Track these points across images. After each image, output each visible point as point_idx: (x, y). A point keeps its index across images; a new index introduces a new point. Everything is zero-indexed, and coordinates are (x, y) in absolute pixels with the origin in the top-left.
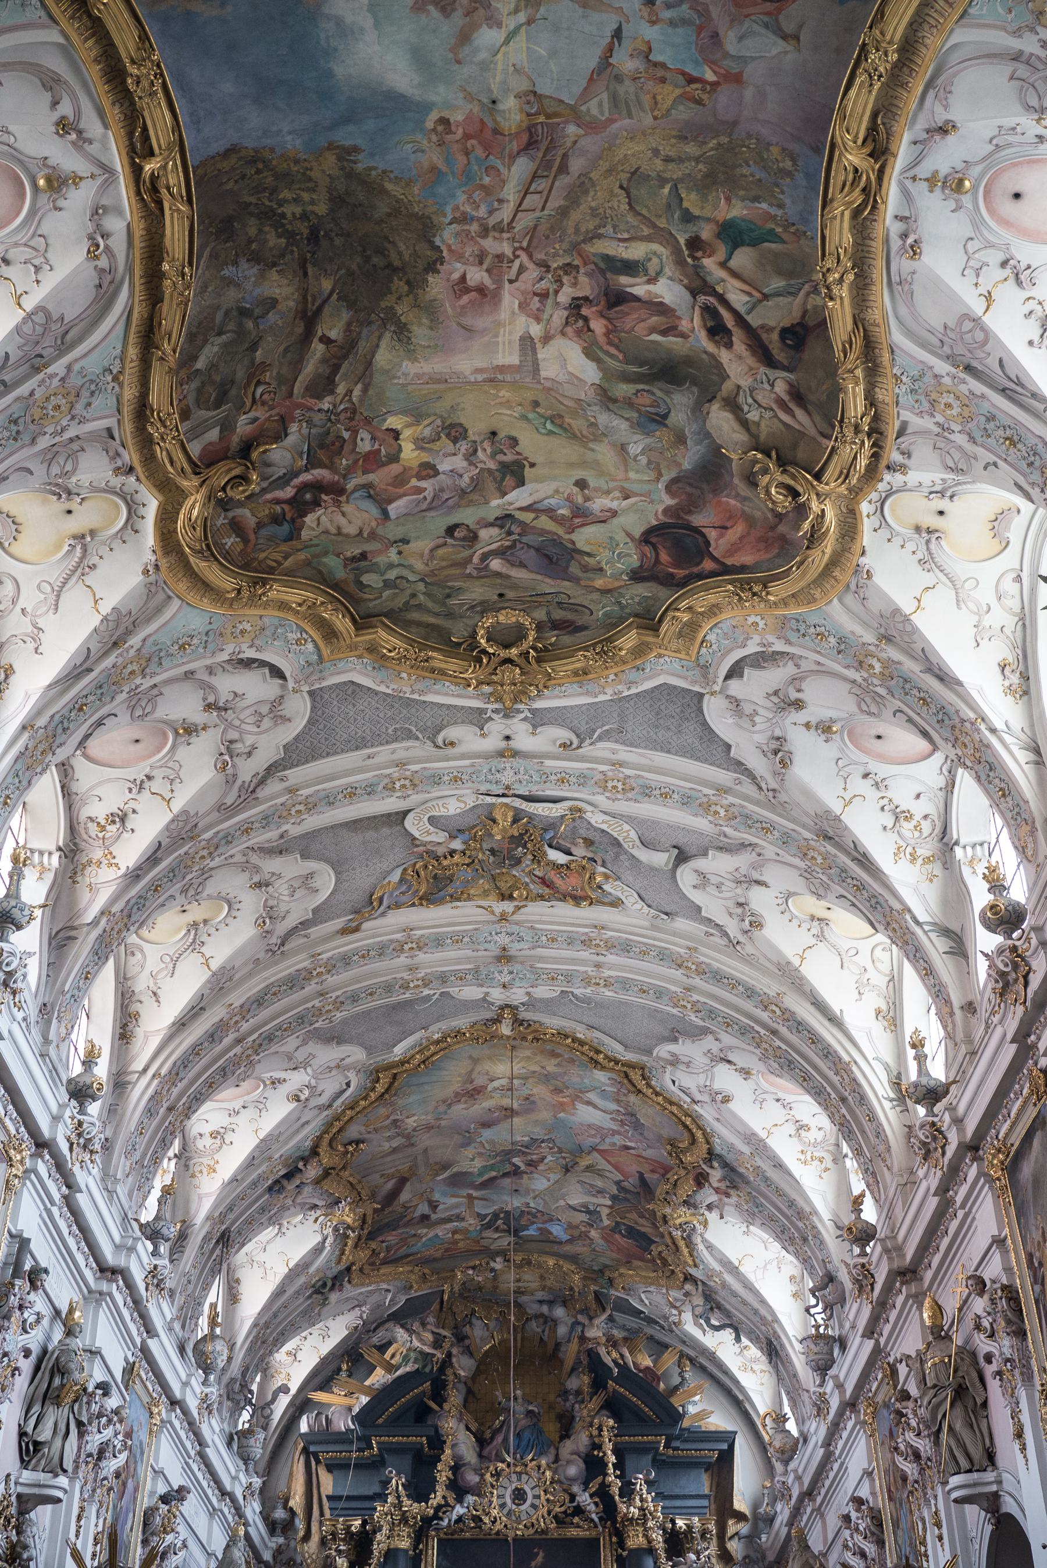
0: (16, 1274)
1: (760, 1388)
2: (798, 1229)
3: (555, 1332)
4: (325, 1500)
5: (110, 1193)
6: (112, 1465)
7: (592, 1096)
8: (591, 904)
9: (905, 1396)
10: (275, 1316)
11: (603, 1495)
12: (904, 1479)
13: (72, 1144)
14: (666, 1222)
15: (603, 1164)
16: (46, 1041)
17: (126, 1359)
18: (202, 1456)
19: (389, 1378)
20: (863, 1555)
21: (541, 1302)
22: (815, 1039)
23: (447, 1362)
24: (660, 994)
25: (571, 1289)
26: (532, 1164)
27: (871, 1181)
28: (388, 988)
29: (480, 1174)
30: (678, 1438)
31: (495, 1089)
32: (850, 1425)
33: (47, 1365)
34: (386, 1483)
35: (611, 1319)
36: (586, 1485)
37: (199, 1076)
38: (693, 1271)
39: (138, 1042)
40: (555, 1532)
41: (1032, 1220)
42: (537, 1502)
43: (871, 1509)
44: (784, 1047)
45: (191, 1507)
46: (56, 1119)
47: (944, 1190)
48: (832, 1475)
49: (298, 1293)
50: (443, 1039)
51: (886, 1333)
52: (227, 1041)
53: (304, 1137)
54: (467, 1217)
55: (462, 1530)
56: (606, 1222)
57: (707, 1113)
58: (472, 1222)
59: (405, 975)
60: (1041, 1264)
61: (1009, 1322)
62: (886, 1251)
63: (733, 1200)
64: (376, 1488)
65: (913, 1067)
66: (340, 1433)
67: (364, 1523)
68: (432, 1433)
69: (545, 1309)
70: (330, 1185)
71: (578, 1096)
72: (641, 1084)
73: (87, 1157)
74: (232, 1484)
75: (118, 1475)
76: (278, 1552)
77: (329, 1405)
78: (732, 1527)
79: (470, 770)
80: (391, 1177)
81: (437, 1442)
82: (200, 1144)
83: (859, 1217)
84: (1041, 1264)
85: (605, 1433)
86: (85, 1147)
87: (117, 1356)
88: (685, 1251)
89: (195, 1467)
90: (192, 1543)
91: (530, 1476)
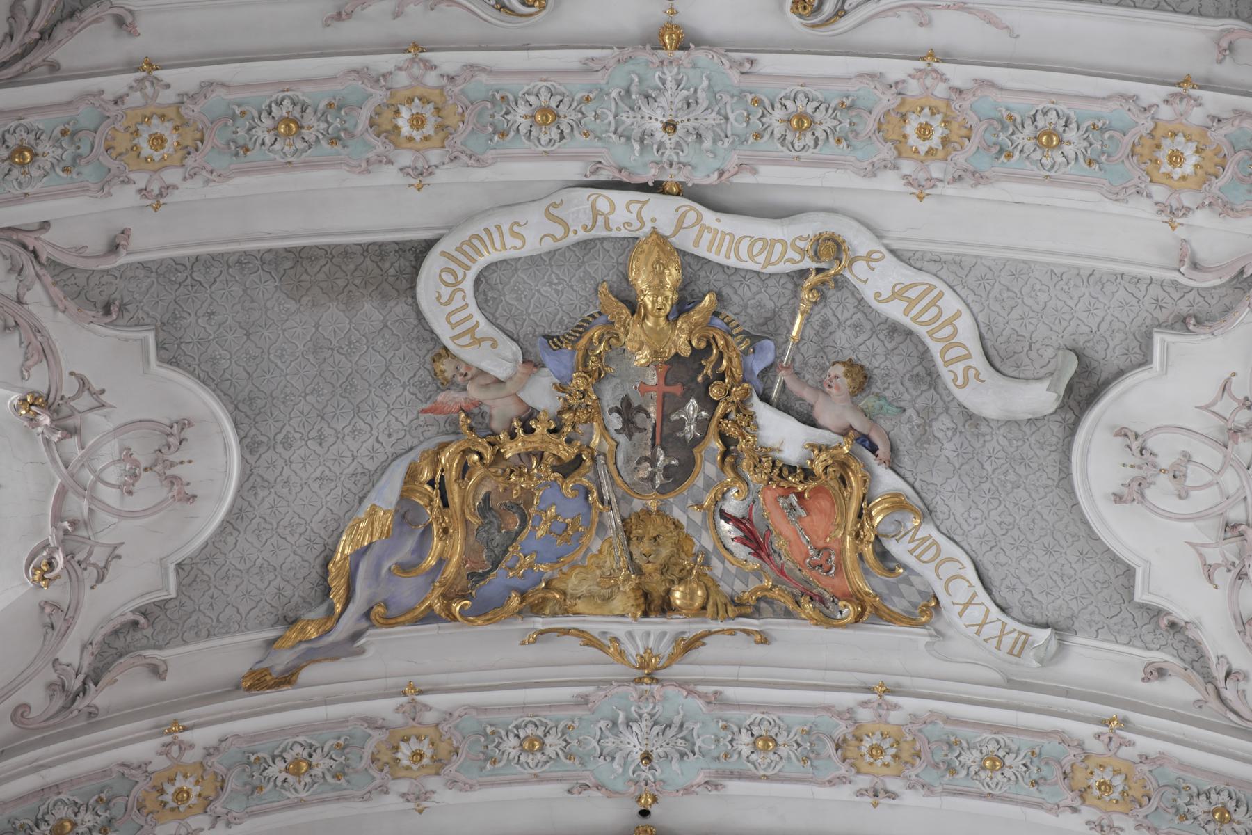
8: (858, 618)
79: (578, 87)
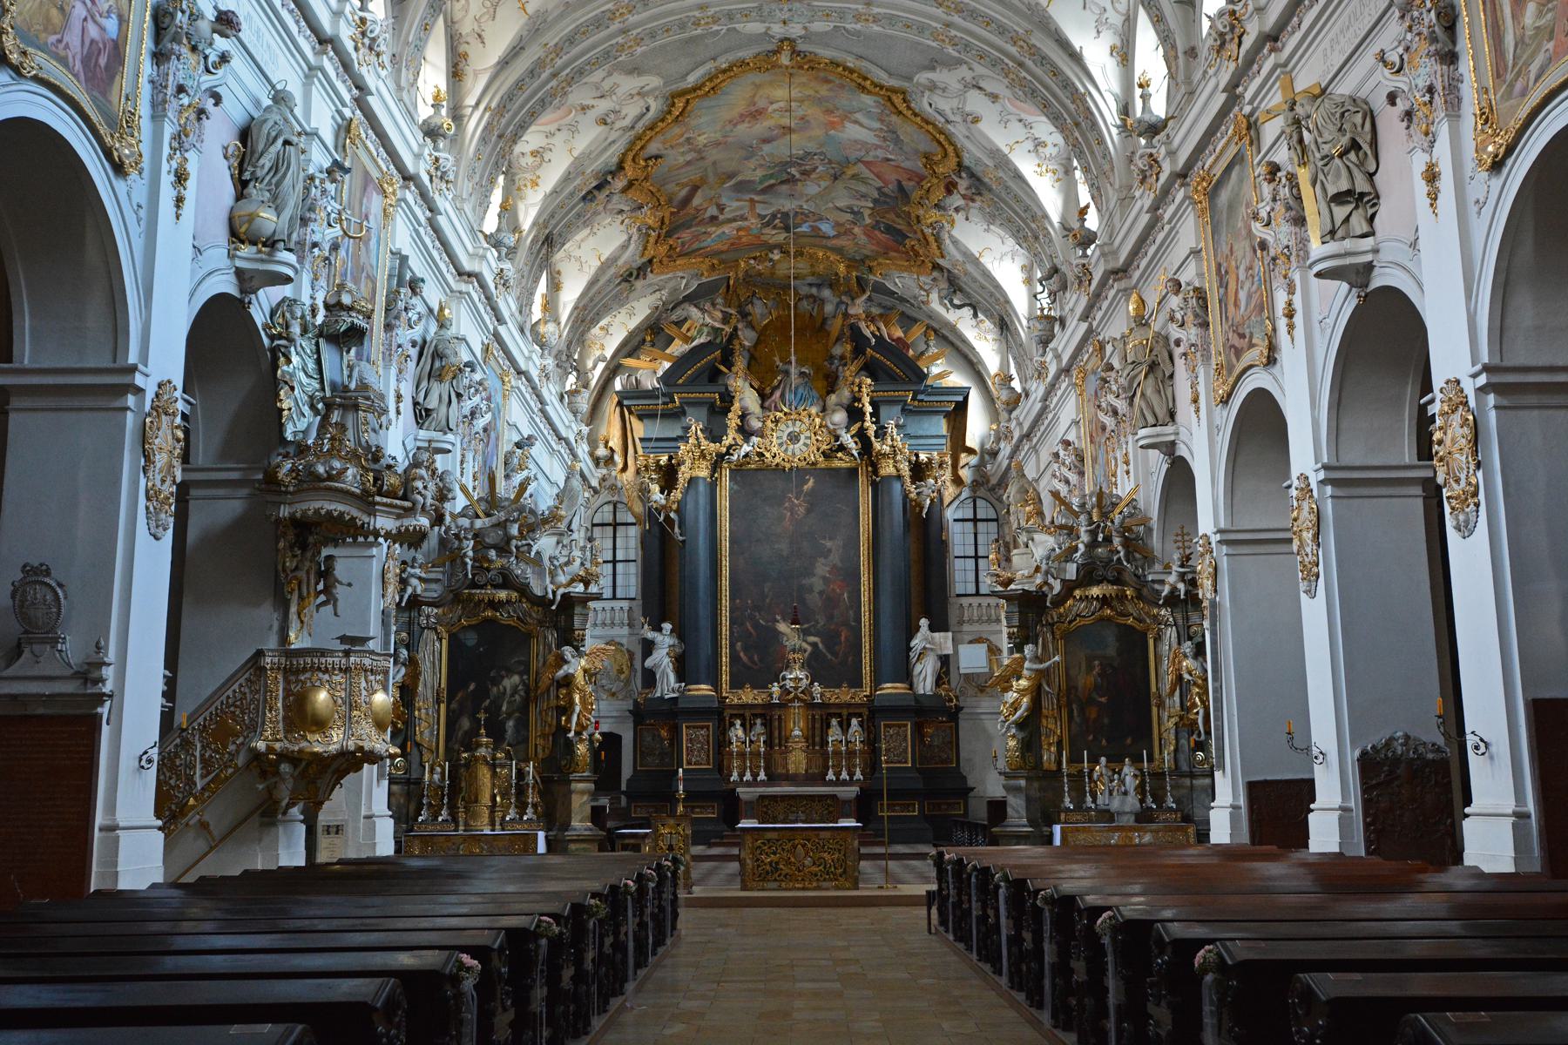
0: (400, 284)
2: (1031, 230)
3: (823, 309)
5: (459, 210)
6: (480, 423)
7: (859, 116)
9: (1110, 368)
10: (591, 300)
11: (862, 436)
12: (1104, 428)
13: (431, 177)
14: (919, 222)
15: (866, 173)
16: (399, 88)
17: (483, 344)
18: (543, 411)
19: (687, 347)
20: (1067, 482)
21: (811, 285)
22: (1056, 72)
23: (734, 335)
24: (921, 29)
25: (837, 274)
26: (804, 173)
27: (1096, 194)
28: (682, 26)
29: (761, 182)
30: (922, 392)
31: (775, 110)
32: (1064, 386)
33: (428, 352)
34: (687, 429)
35: (870, 299)
36: (848, 429)
37: (522, 107)
38: (940, 261)
39: (468, 80)
41: (1223, 237)
42: (808, 442)
43: (1076, 449)
44: (1029, 78)
45: (537, 450)
46: (418, 156)
47: (1155, 208)
48: (1046, 422)
49: (609, 281)
50: (730, 69)
51: (1098, 317)
52: (544, 76)
53: (611, 157)
56: (868, 221)
57: (958, 131)
59: (697, 13)
60: (1227, 272)
61: (1196, 316)
62: (1103, 254)
63: (978, 204)
64: (679, 432)
65: (1139, 103)
67: (671, 458)
68: (723, 389)
69: (814, 291)
70: (636, 195)
71: (847, 116)
72: (902, 107)
73: (444, 186)
75: (485, 430)
76: (604, 479)
77: (637, 369)
78: (964, 458)
80: (687, 185)
81: (728, 398)
82: (523, 162)
83: (1082, 226)
84: (1227, 272)
85: (864, 390)
86: (441, 178)
87: (476, 340)
88: (934, 245)
89: (538, 420)
90: (540, 476)
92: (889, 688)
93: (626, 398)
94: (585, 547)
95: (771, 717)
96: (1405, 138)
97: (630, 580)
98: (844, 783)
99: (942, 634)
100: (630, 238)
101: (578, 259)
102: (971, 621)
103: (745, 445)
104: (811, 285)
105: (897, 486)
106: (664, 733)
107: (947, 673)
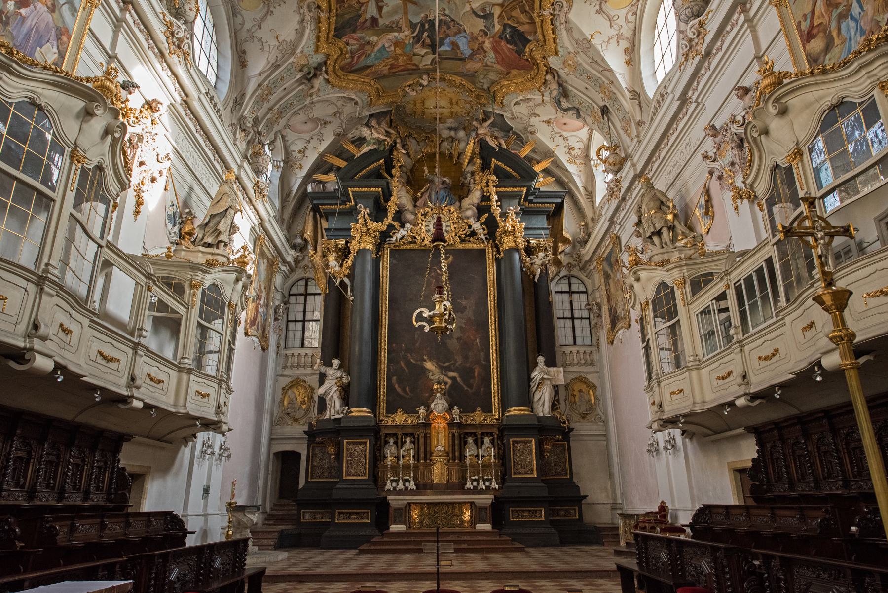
1: (579, 173)
4: (324, 231)
21: (450, 129)
23: (393, 147)
38: (553, 62)
40: (459, 246)
42: (448, 229)
54: (404, 28)
55: (404, 244)
56: (498, 27)
58: (407, 33)
66: (331, 192)
67: (347, 243)
69: (452, 133)
74: (239, 170)
76: (297, 261)
78: (561, 246)
81: (387, 194)
85: (491, 184)
91: (444, 216)
92: (514, 411)
93: (315, 199)
94: (279, 306)
95: (419, 435)
96: (719, 187)
97: (314, 335)
98: (481, 492)
99: (555, 368)
100: (302, 21)
101: (260, 40)
102: (572, 364)
103: (402, 230)
104: (450, 129)
105: (517, 256)
106: (331, 450)
107: (558, 400)
